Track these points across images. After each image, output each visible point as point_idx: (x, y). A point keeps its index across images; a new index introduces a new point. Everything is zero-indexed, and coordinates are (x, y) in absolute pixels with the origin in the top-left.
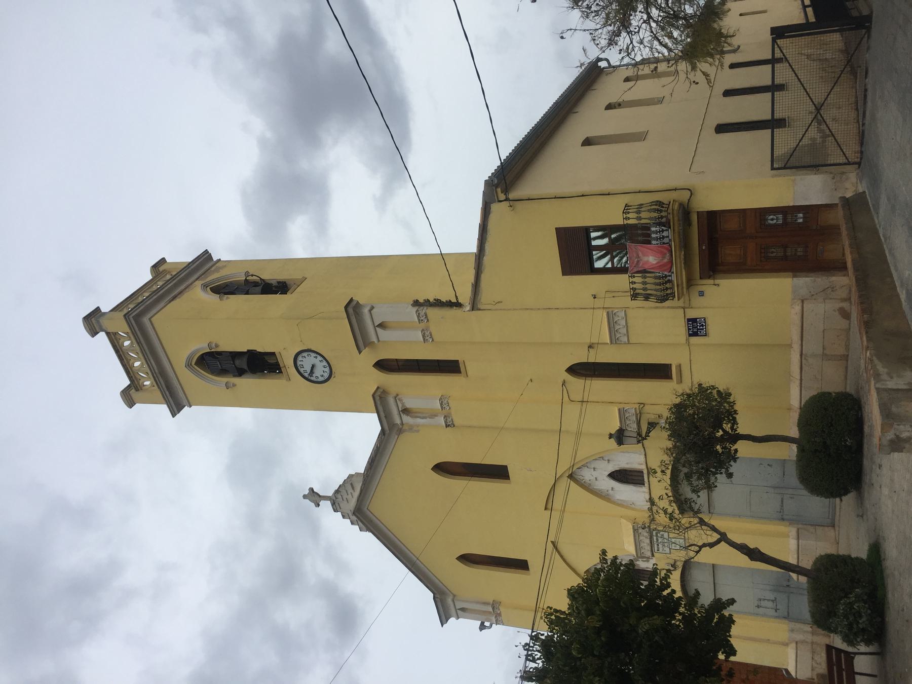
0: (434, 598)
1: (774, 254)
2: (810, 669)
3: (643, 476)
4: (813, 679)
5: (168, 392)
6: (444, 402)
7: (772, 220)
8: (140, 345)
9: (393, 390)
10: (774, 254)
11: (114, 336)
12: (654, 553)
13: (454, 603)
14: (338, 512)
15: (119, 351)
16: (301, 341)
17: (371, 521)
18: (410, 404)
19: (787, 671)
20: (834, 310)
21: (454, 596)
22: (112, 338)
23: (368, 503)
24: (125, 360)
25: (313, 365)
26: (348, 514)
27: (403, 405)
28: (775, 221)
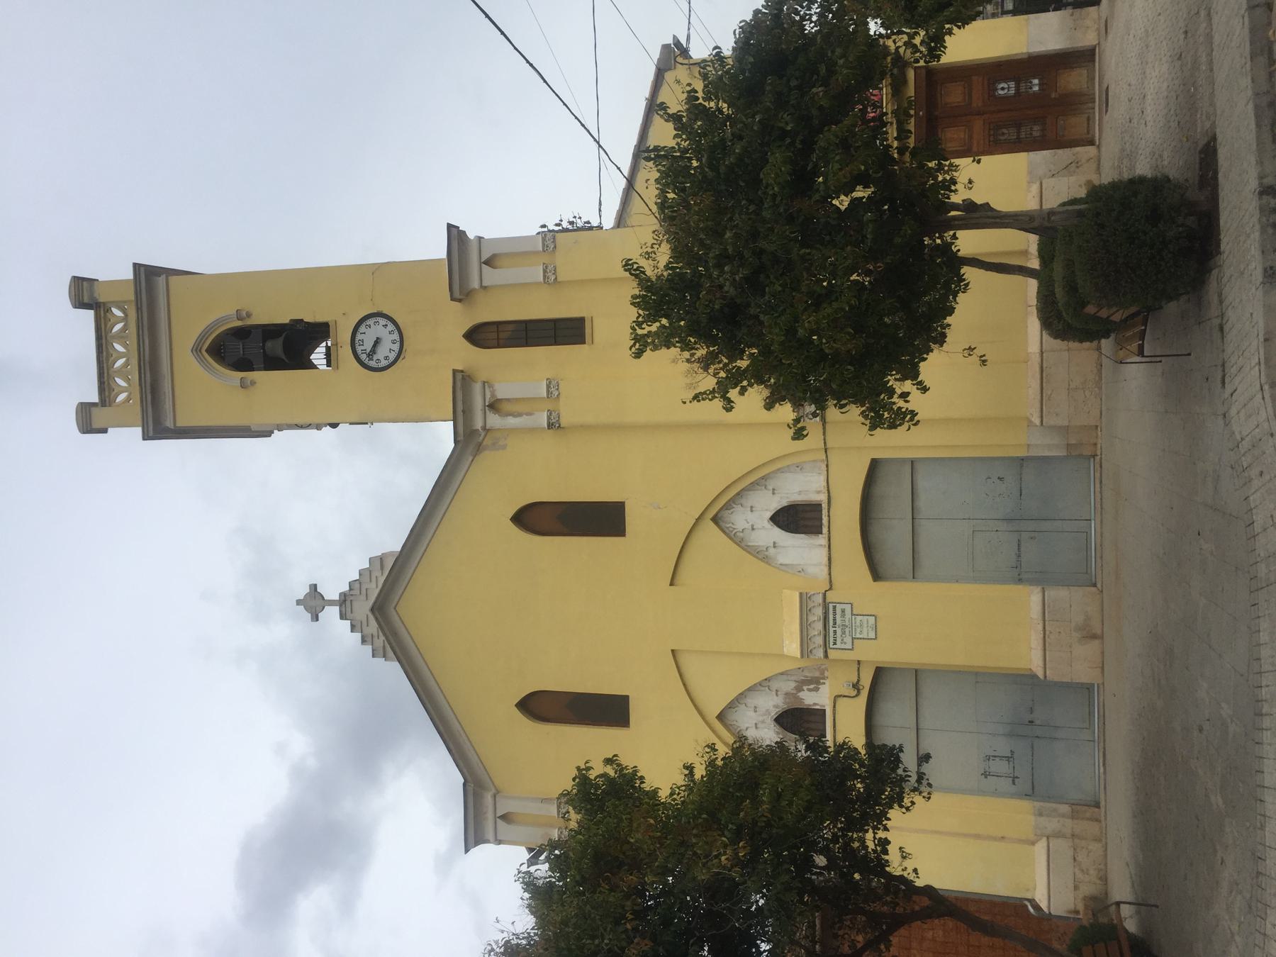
0: (465, 785)
1: (1006, 137)
2: (1071, 885)
3: (821, 519)
4: (1077, 912)
5: (152, 395)
7: (1003, 89)
8: (140, 313)
9: (483, 376)
10: (1006, 137)
11: (105, 313)
12: (828, 650)
13: (495, 800)
14: (346, 619)
15: (102, 339)
19: (1032, 901)
20: (1080, 186)
22: (100, 316)
23: (396, 600)
24: (105, 353)
25: (378, 338)
27: (493, 395)
28: (1006, 91)
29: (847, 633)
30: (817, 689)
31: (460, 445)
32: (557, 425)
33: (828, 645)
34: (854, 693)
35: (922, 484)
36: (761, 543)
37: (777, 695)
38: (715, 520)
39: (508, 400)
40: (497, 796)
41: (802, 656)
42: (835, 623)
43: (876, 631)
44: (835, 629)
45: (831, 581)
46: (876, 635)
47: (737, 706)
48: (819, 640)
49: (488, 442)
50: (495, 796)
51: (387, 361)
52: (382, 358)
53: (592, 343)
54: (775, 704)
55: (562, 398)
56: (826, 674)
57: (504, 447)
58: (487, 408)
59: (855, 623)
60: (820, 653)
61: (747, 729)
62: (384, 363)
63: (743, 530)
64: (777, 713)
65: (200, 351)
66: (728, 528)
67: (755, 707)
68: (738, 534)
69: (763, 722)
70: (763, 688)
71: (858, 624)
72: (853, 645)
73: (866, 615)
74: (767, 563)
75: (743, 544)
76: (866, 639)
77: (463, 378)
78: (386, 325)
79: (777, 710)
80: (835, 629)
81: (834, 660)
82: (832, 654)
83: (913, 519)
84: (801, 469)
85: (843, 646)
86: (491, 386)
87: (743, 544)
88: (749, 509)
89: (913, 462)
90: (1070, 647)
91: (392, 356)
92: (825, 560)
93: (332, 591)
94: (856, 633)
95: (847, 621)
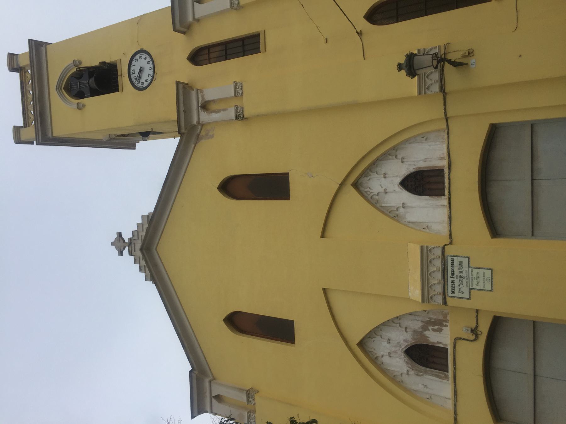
0: (191, 372)
3: (444, 183)
6: (238, 87)
12: (447, 298)
14: (132, 255)
17: (156, 266)
18: (209, 95)
21: (214, 379)
24: (25, 97)
26: (139, 257)
27: (203, 99)
29: (464, 284)
30: (440, 330)
32: (242, 116)
33: (446, 294)
34: (473, 337)
35: (542, 146)
36: (393, 204)
37: (406, 331)
38: (356, 185)
39: (214, 101)
40: (212, 382)
41: (423, 301)
42: (453, 274)
43: (492, 284)
44: (453, 279)
45: (451, 237)
46: (492, 287)
48: (439, 289)
49: (203, 133)
50: (210, 382)
51: (147, 83)
52: (144, 81)
53: (265, 51)
54: (405, 338)
55: (244, 94)
56: (448, 318)
57: (212, 136)
59: (472, 275)
60: (439, 299)
61: (382, 356)
62: (146, 84)
63: (378, 193)
64: (406, 346)
65: (61, 89)
66: (366, 192)
67: (389, 340)
68: (374, 197)
69: (395, 352)
70: (395, 325)
71: (475, 275)
72: (470, 295)
73: (482, 268)
74: (398, 221)
75: (378, 205)
77: (184, 88)
78: (146, 58)
79: (407, 344)
80: (453, 279)
81: (453, 307)
82: (450, 301)
83: (532, 179)
84: (426, 140)
85: (461, 295)
86: (202, 92)
87: (378, 205)
88: (382, 176)
89: (533, 126)
91: (150, 79)
92: (446, 219)
93: (127, 236)
94: (472, 284)
95: (464, 272)
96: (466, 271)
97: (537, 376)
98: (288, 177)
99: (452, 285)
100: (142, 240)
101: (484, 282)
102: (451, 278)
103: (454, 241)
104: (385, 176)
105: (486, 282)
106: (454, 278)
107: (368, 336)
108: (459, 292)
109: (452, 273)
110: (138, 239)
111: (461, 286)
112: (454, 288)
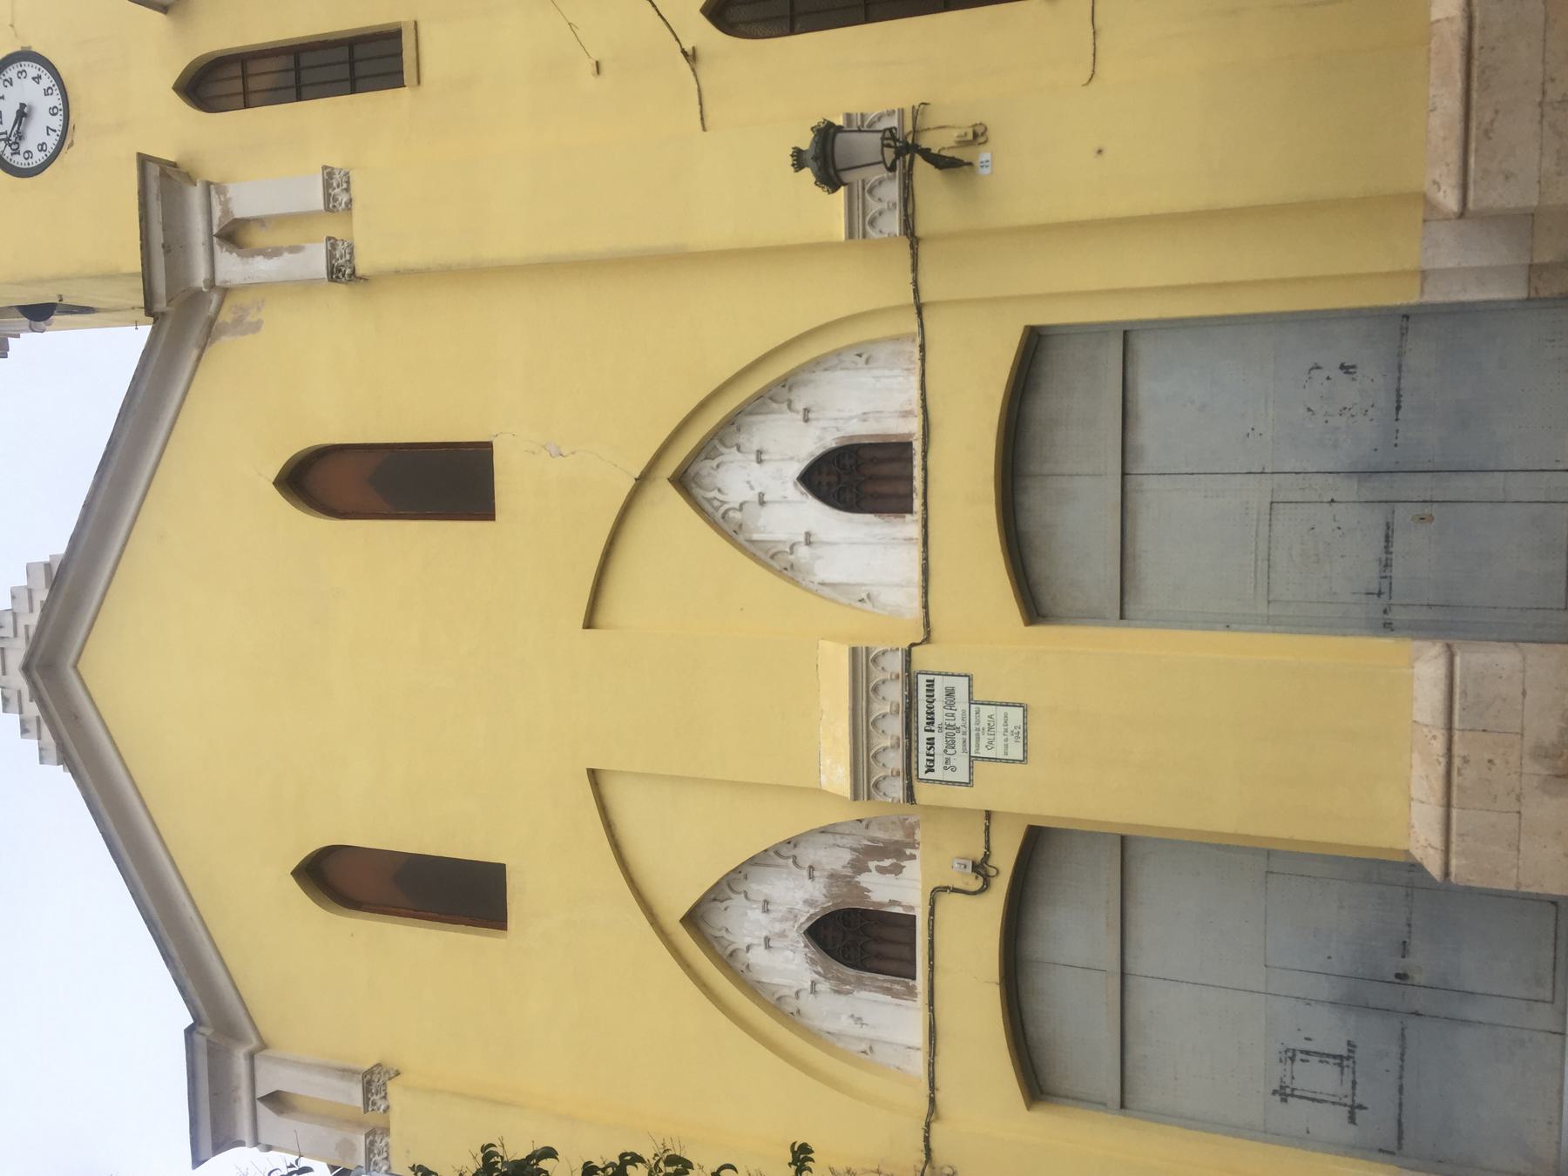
0: (189, 1032)
3: (910, 478)
6: (335, 185)
12: (916, 784)
16: (12, 26)
17: (73, 718)
18: (245, 203)
21: (264, 1046)
26: (19, 692)
27: (226, 211)
29: (959, 746)
30: (896, 870)
31: (167, 324)
32: (348, 271)
33: (914, 773)
34: (976, 884)
35: (1147, 389)
36: (780, 535)
37: (811, 877)
38: (683, 481)
39: (261, 221)
40: (257, 1057)
41: (856, 796)
42: (931, 721)
44: (930, 735)
45: (927, 624)
46: (1025, 751)
47: (730, 898)
48: (895, 760)
49: (226, 316)
50: (251, 1057)
51: (43, 154)
52: (34, 149)
53: (419, 82)
54: (807, 896)
55: (356, 206)
56: (918, 836)
57: (256, 327)
58: (215, 239)
59: (978, 723)
60: (896, 789)
61: (748, 948)
62: (39, 158)
63: (742, 505)
64: (809, 919)
66: (709, 501)
67: (766, 902)
68: (731, 514)
69: (782, 935)
70: (781, 861)
71: (984, 723)
72: (971, 774)
74: (793, 581)
75: (741, 538)
76: (1000, 760)
77: (164, 175)
78: (39, 77)
79: (812, 911)
80: (930, 735)
81: (927, 807)
82: (923, 793)
83: (1124, 474)
84: (867, 362)
85: (949, 776)
86: (221, 190)
87: (741, 538)
88: (753, 457)
89: (1127, 335)
90: (1518, 798)
91: (52, 142)
92: (917, 576)
94: (978, 746)
95: (958, 715)
96: (964, 712)
97: (1132, 975)
98: (492, 452)
99: (929, 749)
100: (27, 638)
101: (1006, 740)
102: (926, 730)
103: (934, 635)
104: (760, 457)
105: (1012, 739)
106: (933, 731)
107: (713, 896)
108: (945, 768)
109: (928, 719)
110: (16, 634)
111: (950, 751)
112: (932, 758)
